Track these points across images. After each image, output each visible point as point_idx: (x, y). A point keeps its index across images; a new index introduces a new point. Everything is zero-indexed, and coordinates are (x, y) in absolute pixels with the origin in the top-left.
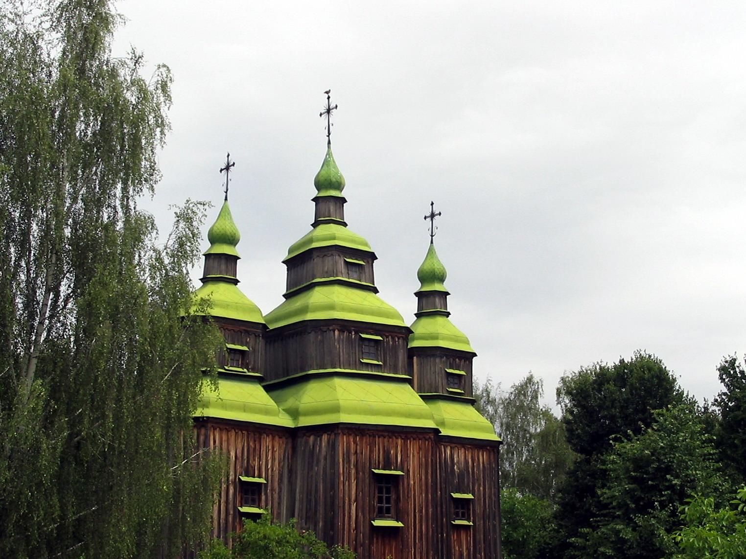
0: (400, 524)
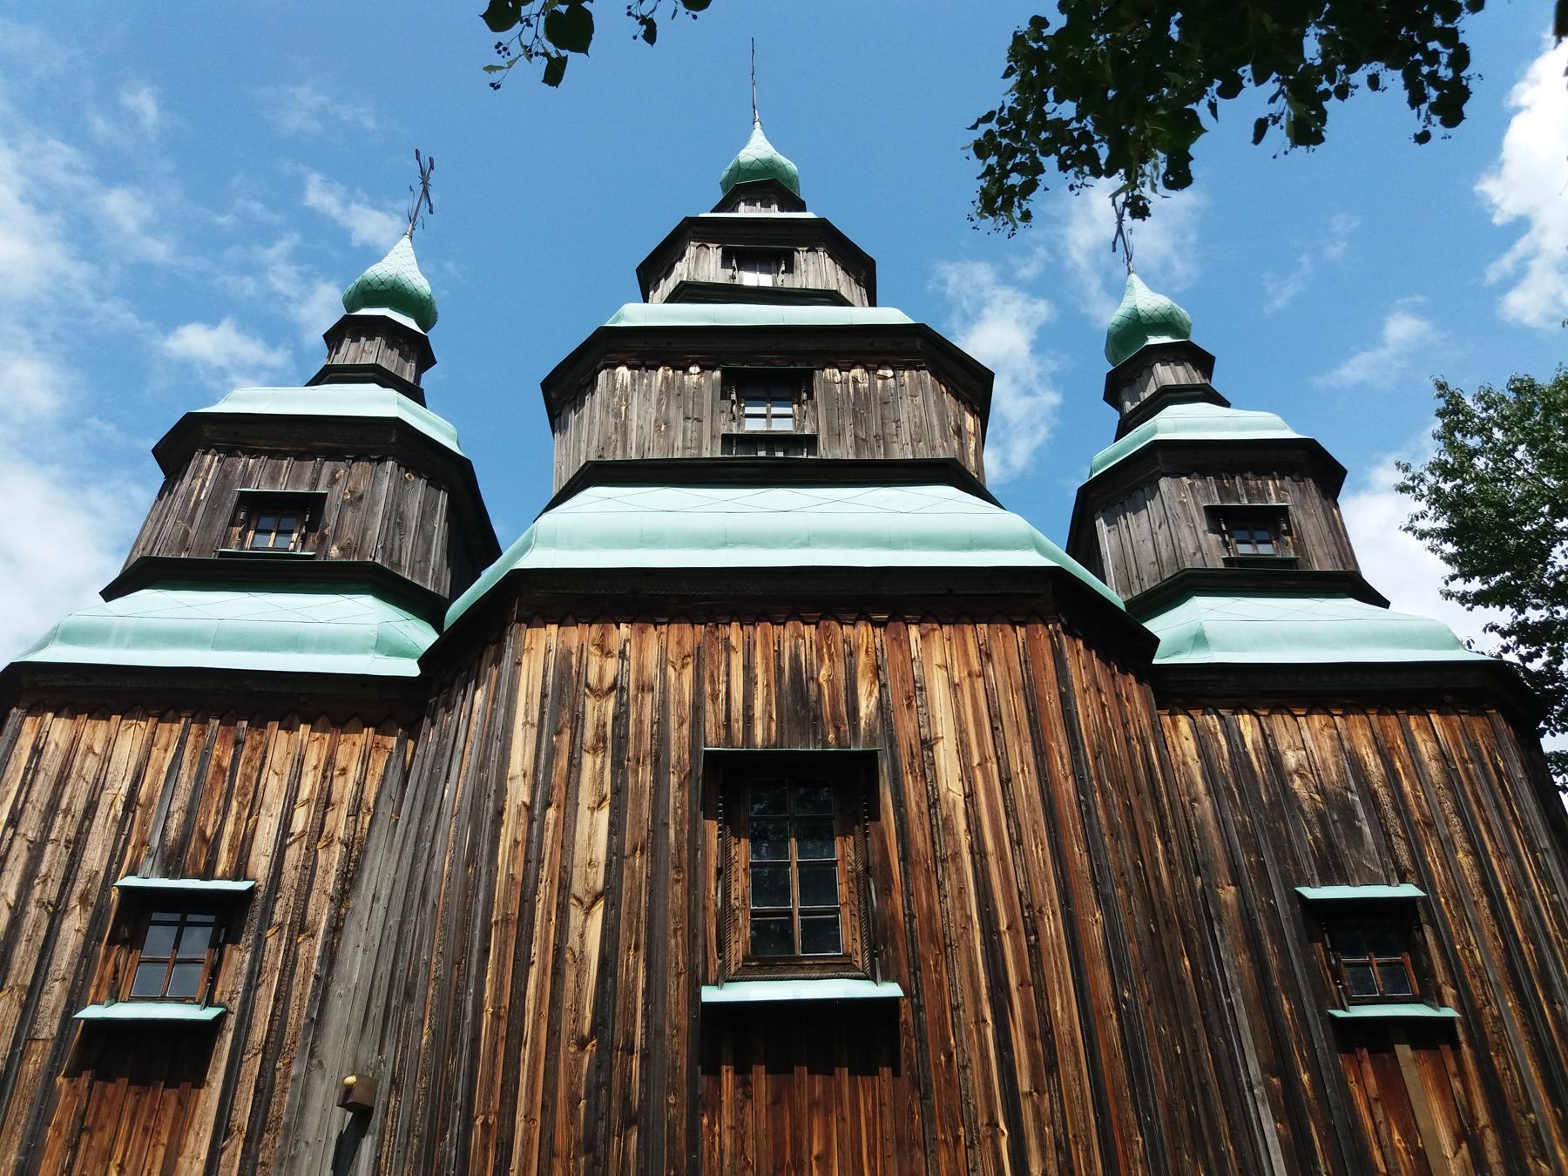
0: (892, 990)
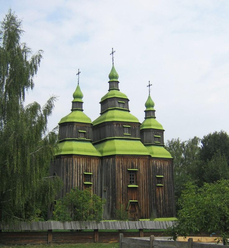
0: (137, 186)
